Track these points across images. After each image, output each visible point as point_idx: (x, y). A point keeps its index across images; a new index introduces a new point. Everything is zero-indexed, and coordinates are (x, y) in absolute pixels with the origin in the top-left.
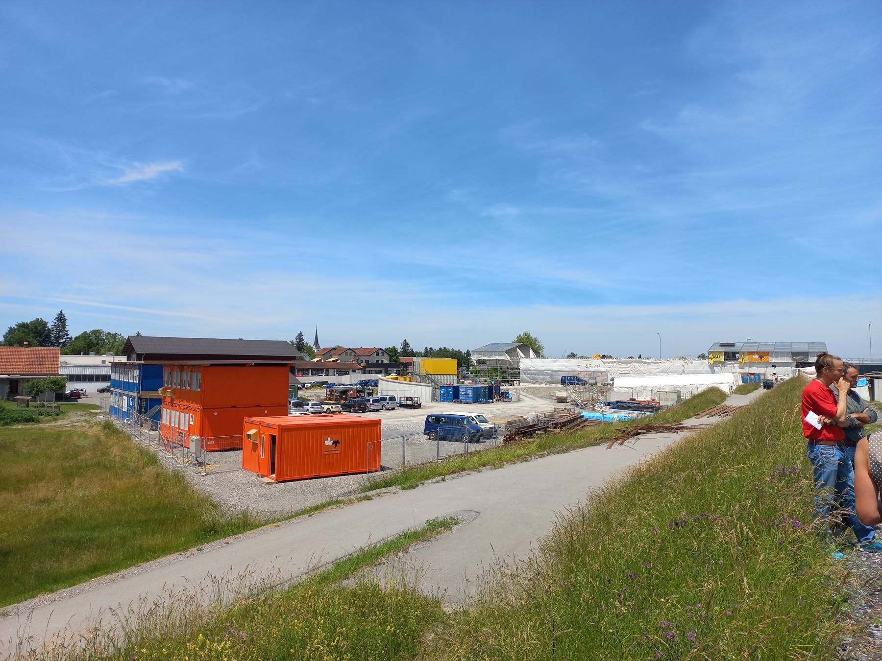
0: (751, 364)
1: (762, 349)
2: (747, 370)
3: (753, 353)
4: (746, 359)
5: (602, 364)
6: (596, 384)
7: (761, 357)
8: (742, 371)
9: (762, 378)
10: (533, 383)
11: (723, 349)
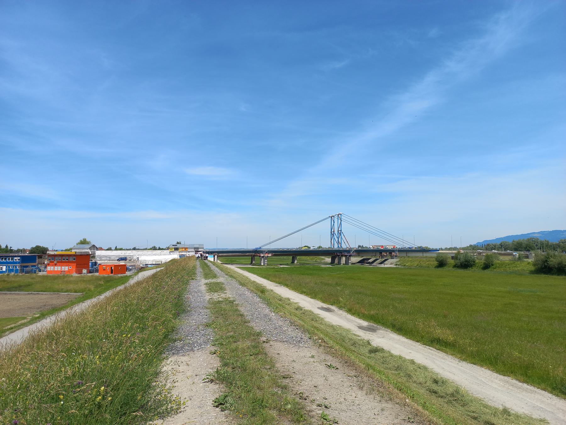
0: (182, 252)
1: (186, 247)
2: (181, 254)
3: (183, 248)
4: (181, 250)
5: (131, 253)
6: (131, 260)
7: (185, 249)
8: (180, 254)
9: (185, 256)
10: (102, 261)
11: (174, 247)
